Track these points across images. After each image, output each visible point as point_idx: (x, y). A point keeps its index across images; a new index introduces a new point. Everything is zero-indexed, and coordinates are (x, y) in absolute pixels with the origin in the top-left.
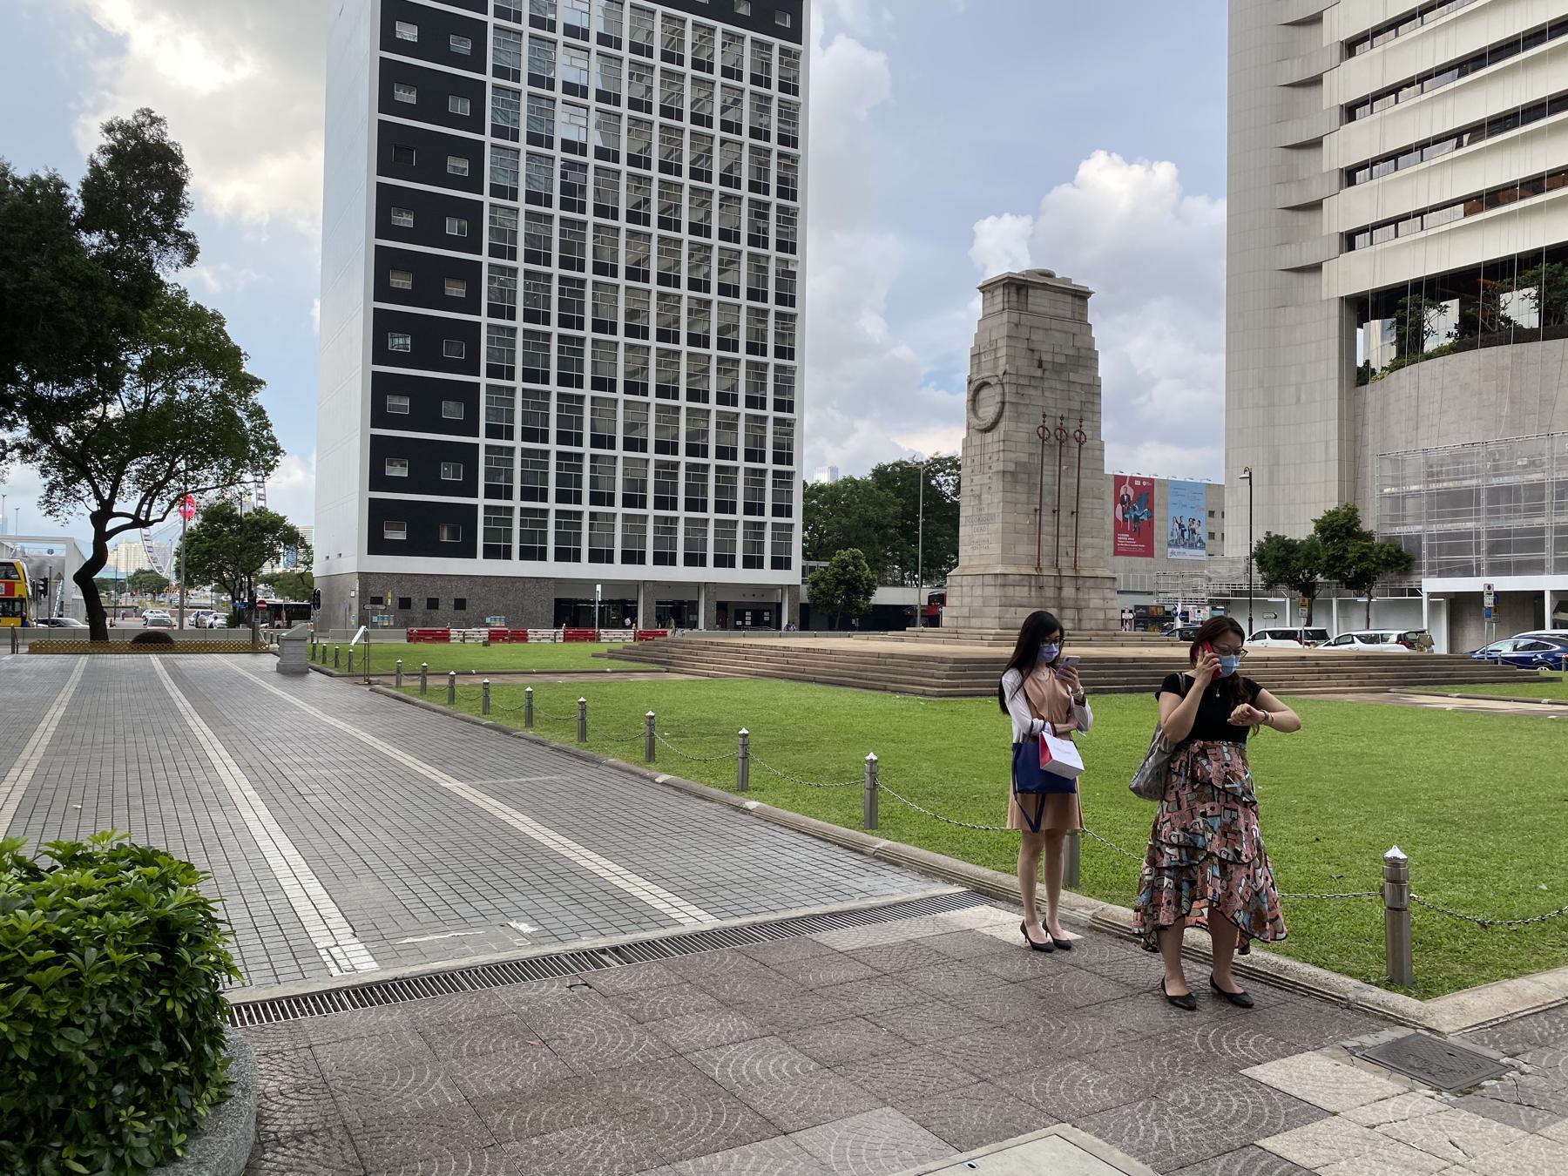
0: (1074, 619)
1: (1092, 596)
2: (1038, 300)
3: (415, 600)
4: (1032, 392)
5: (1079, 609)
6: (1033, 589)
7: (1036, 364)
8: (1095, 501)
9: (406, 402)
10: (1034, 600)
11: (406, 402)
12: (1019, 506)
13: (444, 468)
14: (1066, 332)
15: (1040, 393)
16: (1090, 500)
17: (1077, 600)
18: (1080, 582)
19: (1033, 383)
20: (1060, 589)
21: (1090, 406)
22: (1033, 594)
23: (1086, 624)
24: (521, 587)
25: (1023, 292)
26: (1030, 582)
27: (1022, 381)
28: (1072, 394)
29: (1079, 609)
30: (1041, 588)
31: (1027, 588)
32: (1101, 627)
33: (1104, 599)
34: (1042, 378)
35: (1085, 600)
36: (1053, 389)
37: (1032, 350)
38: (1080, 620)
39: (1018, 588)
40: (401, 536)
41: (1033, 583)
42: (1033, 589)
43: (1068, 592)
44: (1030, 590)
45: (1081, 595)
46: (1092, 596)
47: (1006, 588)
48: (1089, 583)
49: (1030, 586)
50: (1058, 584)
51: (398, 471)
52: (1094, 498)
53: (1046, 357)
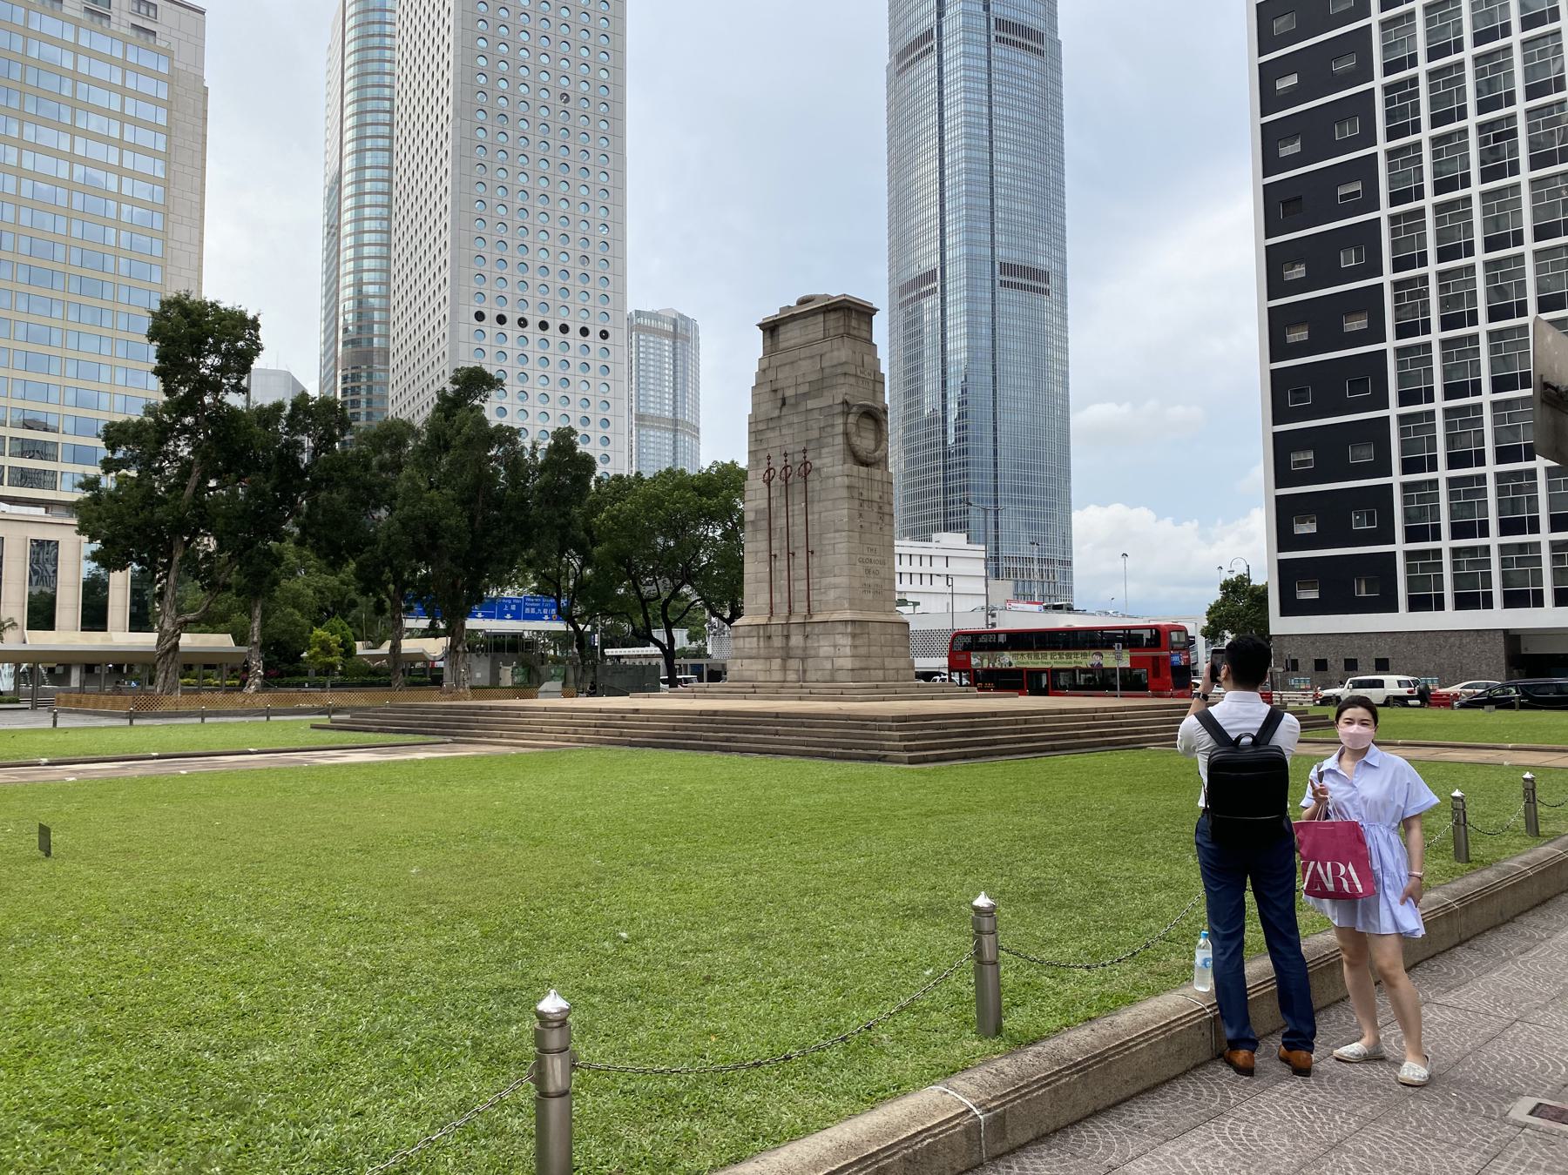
0: (798, 670)
1: (822, 643)
2: (789, 335)
3: (1331, 662)
4: (770, 434)
5: (803, 659)
6: (762, 639)
7: (779, 403)
8: (837, 535)
9: (1310, 456)
10: (762, 651)
11: (1310, 456)
12: (759, 554)
13: (1355, 518)
14: (812, 357)
15: (777, 433)
16: (832, 535)
17: (805, 649)
18: (808, 629)
19: (771, 425)
20: (787, 637)
21: (829, 429)
22: (762, 644)
23: (811, 676)
24: (1458, 643)
25: (776, 334)
26: (759, 633)
27: (761, 426)
28: (810, 423)
29: (803, 659)
30: (770, 637)
31: (755, 639)
32: (828, 678)
33: (835, 646)
34: (779, 417)
35: (813, 647)
36: (790, 425)
37: (775, 391)
38: (805, 671)
39: (747, 639)
40: (1313, 595)
41: (761, 632)
42: (762, 639)
43: (796, 640)
44: (759, 641)
45: (809, 643)
46: (822, 643)
47: (737, 640)
48: (818, 629)
49: (759, 637)
50: (785, 633)
51: (1307, 528)
52: (836, 531)
53: (789, 393)
